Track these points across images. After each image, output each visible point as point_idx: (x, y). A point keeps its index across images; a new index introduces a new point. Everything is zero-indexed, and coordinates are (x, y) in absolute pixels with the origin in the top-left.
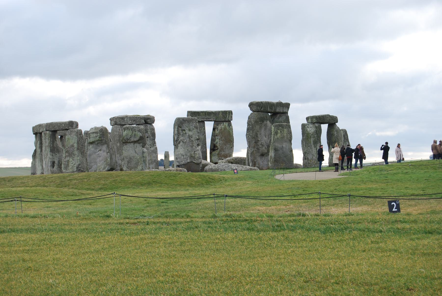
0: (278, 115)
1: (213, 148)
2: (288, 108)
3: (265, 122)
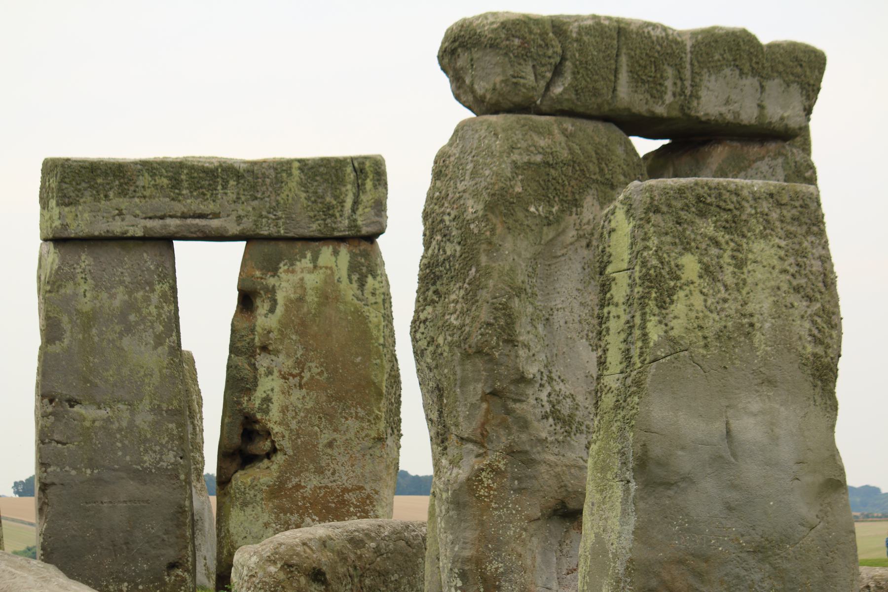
0: (719, 153)
1: (246, 441)
2: (811, 91)
3: (590, 208)
